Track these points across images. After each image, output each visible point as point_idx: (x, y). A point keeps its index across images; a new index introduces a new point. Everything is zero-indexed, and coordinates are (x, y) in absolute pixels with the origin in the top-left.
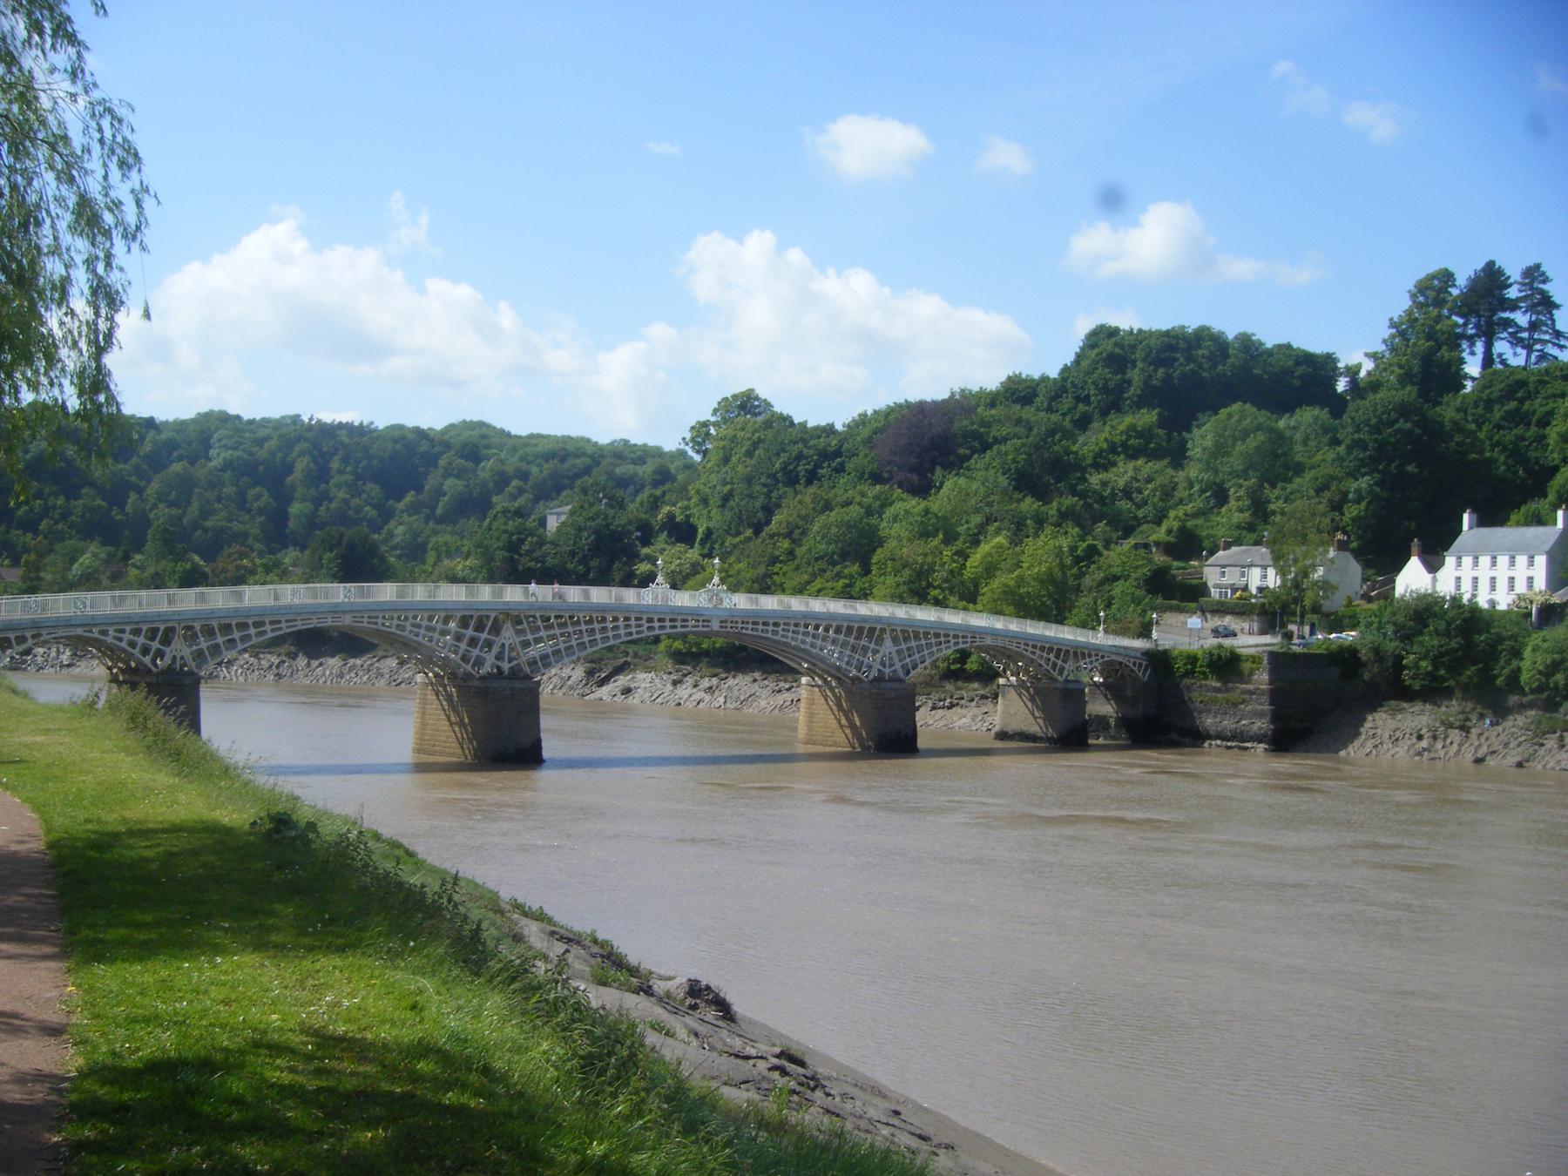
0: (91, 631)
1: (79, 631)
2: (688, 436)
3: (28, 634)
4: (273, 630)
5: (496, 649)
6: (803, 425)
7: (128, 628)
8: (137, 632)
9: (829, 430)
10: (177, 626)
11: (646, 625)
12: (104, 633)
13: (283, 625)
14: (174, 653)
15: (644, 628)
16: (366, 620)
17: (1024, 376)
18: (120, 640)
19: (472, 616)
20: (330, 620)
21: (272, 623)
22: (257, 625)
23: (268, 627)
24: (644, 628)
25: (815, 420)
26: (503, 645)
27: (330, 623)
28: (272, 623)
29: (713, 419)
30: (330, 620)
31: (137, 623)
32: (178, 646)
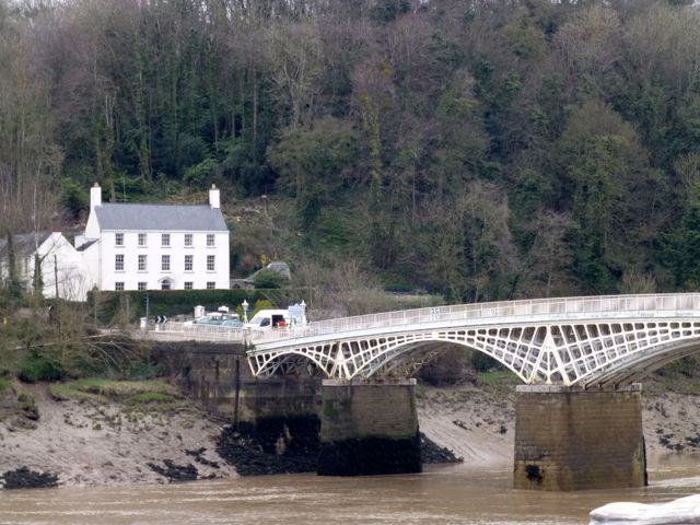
1: (292, 351)
4: (390, 345)
5: (539, 359)
8: (319, 349)
11: (671, 330)
12: (304, 350)
13: (405, 339)
15: (669, 334)
16: (447, 335)
19: (521, 329)
20: (414, 337)
21: (390, 340)
22: (382, 341)
23: (396, 341)
24: (669, 334)
27: (424, 339)
28: (390, 340)
30: (414, 337)
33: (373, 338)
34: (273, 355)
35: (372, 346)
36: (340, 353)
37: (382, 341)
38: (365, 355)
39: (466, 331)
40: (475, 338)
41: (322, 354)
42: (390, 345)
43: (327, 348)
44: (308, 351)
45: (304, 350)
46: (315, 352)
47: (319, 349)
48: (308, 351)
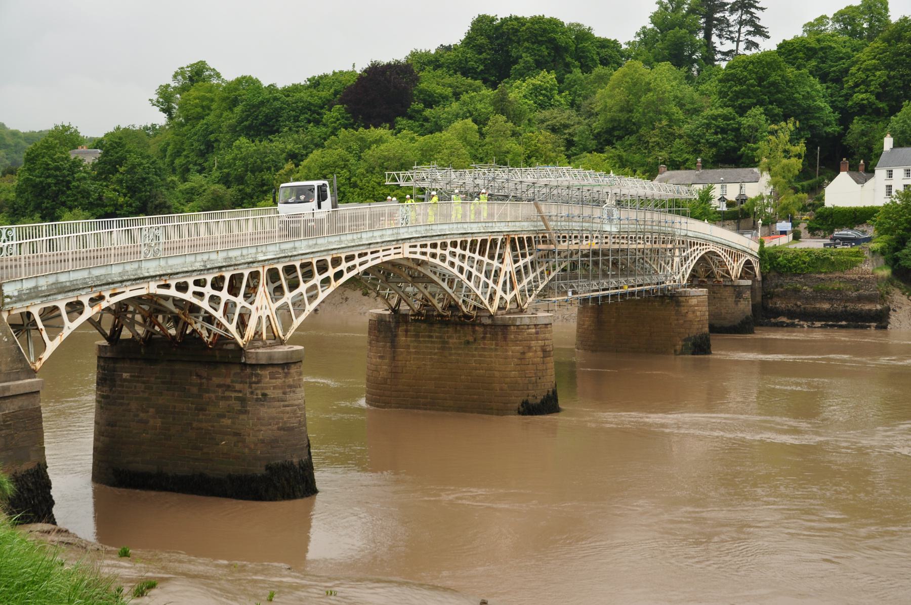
0: (167, 286)
1: (152, 288)
2: (155, 97)
3: (85, 300)
4: (349, 269)
6: (272, 88)
7: (209, 278)
9: (296, 88)
10: (260, 270)
14: (260, 313)
17: (423, 51)
18: (200, 295)
25: (282, 83)
26: (506, 272)
29: (173, 84)
31: (220, 268)
32: (265, 303)
33: (335, 254)
34: (93, 301)
35: (334, 267)
36: (263, 291)
37: (336, 262)
38: (308, 290)
39: (418, 244)
40: (447, 253)
41: (224, 295)
42: (349, 269)
43: (236, 280)
44: (192, 288)
45: (182, 287)
46: (208, 291)
47: (217, 284)
48: (192, 288)
